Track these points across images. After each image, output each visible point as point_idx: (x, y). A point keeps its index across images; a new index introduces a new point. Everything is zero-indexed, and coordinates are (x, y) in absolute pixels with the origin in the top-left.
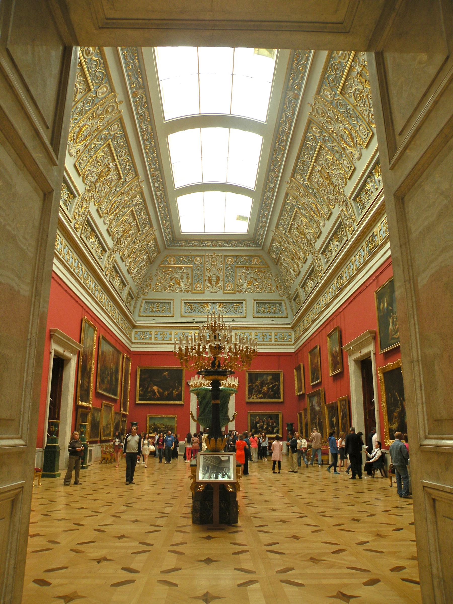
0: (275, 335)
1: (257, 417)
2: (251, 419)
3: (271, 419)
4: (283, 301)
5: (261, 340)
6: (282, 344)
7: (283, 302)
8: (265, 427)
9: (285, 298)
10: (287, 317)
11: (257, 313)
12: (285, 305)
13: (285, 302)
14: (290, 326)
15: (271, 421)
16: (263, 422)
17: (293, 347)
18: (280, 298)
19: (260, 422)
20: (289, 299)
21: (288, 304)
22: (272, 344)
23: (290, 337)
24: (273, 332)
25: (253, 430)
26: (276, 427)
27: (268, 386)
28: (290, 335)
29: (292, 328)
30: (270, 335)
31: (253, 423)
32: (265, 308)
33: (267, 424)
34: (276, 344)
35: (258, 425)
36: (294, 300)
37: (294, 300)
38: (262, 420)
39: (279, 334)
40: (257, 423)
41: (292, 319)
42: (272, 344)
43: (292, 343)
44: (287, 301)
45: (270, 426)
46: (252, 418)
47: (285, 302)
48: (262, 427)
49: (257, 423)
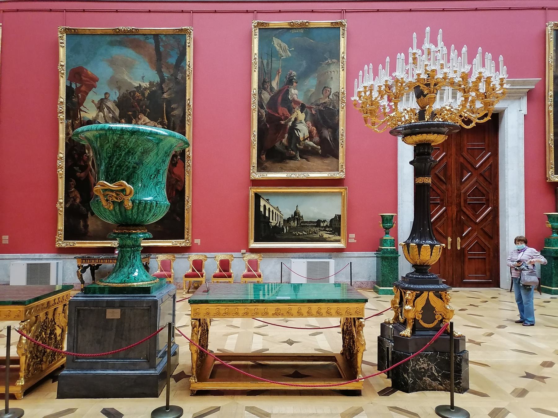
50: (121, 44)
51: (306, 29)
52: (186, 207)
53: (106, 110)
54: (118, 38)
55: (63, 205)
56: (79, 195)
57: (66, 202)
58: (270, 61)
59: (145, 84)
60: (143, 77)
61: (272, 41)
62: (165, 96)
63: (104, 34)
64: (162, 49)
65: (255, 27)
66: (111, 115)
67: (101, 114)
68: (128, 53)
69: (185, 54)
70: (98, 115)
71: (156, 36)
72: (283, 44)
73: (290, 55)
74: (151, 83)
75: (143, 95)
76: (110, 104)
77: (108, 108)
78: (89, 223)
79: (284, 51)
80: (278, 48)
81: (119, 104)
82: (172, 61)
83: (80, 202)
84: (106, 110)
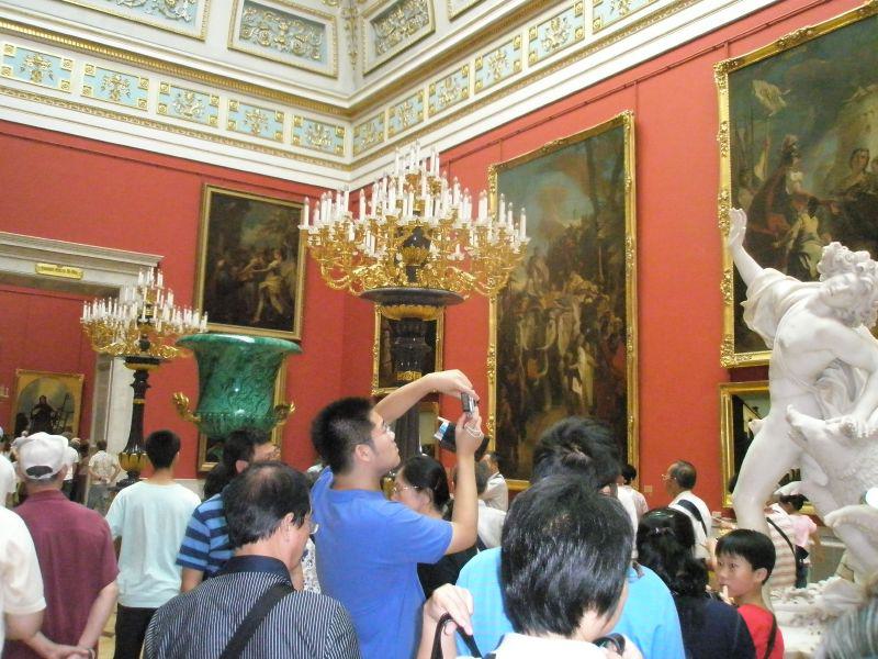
0: (297, 125)
4: (329, 18)
5: (248, 129)
6: (315, 160)
7: (329, 25)
9: (338, 12)
10: (334, 77)
11: (241, 37)
12: (336, 34)
13: (335, 29)
14: (347, 105)
17: (348, 175)
18: (325, 10)
20: (351, 17)
21: (343, 34)
22: (287, 154)
23: (339, 141)
24: (290, 115)
28: (340, 136)
29: (351, 114)
30: (280, 121)
32: (269, 29)
34: (296, 156)
36: (378, 21)
37: (378, 21)
39: (307, 124)
41: (344, 92)
42: (287, 154)
43: (348, 159)
44: (342, 24)
47: (335, 24)
50: (550, 168)
51: (810, 44)
52: (629, 426)
53: (535, 273)
54: (548, 160)
55: (494, 424)
56: (509, 410)
57: (498, 420)
58: (750, 127)
59: (577, 223)
60: (574, 212)
61: (751, 88)
62: (601, 235)
63: (533, 158)
64: (595, 159)
65: (721, 73)
66: (541, 281)
67: (531, 281)
68: (557, 179)
69: (623, 159)
70: (527, 283)
71: (587, 139)
72: (772, 89)
73: (783, 103)
74: (584, 220)
75: (574, 238)
76: (540, 264)
77: (538, 270)
78: (520, 452)
79: (774, 100)
80: (762, 98)
81: (548, 263)
82: (608, 175)
83: (513, 420)
84: (535, 273)
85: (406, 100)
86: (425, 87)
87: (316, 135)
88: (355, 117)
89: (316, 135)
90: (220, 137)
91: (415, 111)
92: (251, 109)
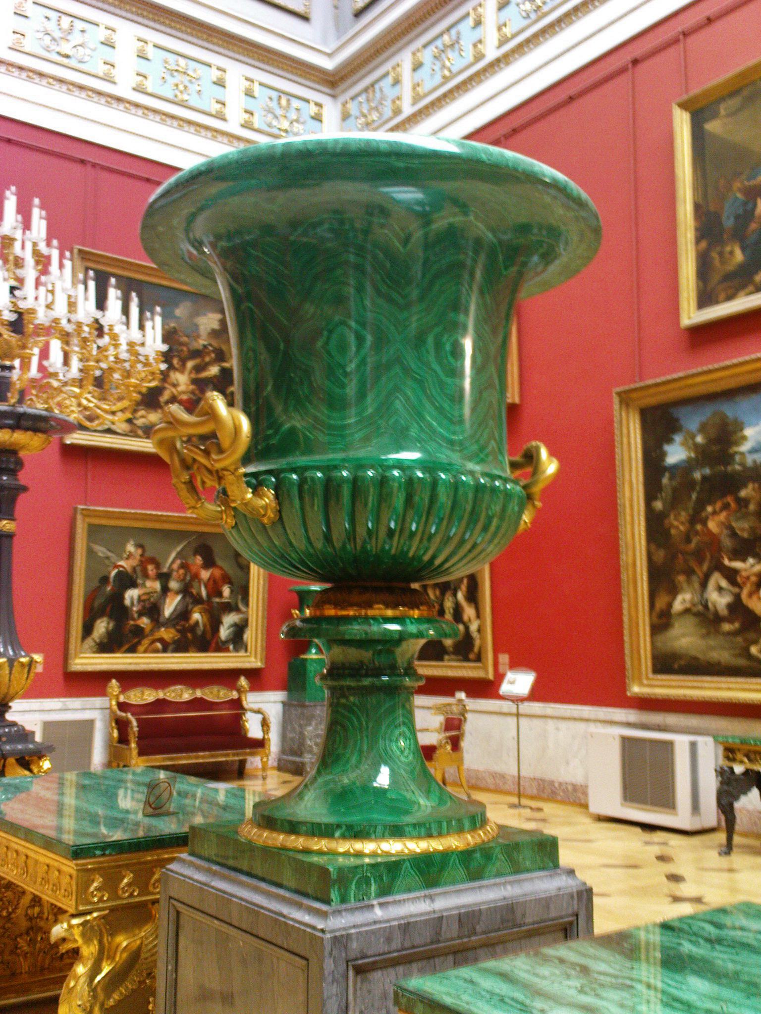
1: (130, 548)
2: (90, 552)
3: (209, 563)
8: (169, 608)
15: (205, 575)
16: (164, 578)
19: (146, 576)
25: (102, 627)
26: (229, 608)
27: (199, 369)
31: (105, 580)
33: (186, 591)
35: (132, 595)
38: (158, 566)
40: (127, 581)
45: (198, 600)
46: (101, 551)
48: (152, 610)
49: (127, 581)
85: (448, 30)
86: (405, 59)
87: (279, 112)
88: (343, 86)
89: (279, 112)
90: (119, 100)
91: (467, 43)
92: (171, 58)
